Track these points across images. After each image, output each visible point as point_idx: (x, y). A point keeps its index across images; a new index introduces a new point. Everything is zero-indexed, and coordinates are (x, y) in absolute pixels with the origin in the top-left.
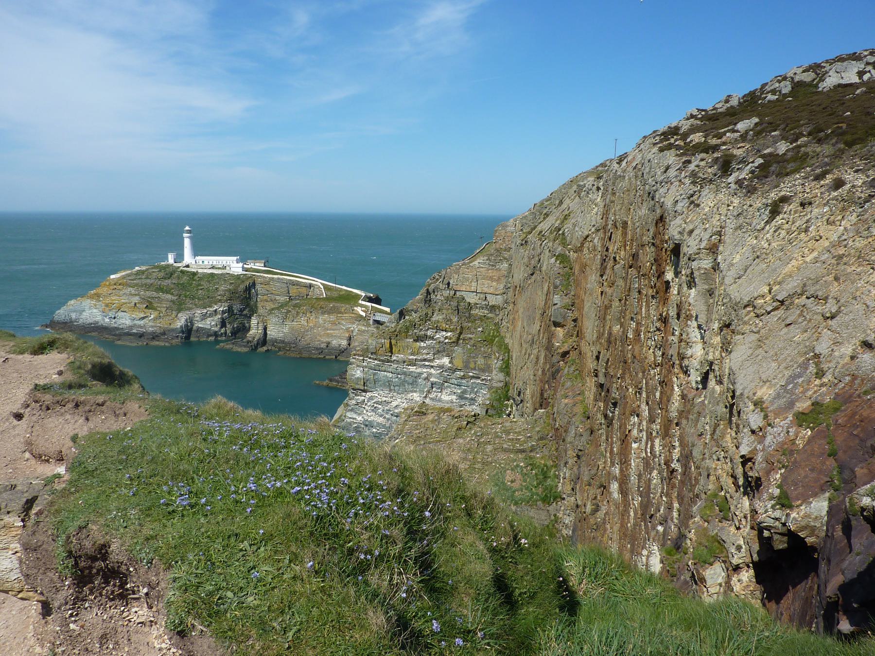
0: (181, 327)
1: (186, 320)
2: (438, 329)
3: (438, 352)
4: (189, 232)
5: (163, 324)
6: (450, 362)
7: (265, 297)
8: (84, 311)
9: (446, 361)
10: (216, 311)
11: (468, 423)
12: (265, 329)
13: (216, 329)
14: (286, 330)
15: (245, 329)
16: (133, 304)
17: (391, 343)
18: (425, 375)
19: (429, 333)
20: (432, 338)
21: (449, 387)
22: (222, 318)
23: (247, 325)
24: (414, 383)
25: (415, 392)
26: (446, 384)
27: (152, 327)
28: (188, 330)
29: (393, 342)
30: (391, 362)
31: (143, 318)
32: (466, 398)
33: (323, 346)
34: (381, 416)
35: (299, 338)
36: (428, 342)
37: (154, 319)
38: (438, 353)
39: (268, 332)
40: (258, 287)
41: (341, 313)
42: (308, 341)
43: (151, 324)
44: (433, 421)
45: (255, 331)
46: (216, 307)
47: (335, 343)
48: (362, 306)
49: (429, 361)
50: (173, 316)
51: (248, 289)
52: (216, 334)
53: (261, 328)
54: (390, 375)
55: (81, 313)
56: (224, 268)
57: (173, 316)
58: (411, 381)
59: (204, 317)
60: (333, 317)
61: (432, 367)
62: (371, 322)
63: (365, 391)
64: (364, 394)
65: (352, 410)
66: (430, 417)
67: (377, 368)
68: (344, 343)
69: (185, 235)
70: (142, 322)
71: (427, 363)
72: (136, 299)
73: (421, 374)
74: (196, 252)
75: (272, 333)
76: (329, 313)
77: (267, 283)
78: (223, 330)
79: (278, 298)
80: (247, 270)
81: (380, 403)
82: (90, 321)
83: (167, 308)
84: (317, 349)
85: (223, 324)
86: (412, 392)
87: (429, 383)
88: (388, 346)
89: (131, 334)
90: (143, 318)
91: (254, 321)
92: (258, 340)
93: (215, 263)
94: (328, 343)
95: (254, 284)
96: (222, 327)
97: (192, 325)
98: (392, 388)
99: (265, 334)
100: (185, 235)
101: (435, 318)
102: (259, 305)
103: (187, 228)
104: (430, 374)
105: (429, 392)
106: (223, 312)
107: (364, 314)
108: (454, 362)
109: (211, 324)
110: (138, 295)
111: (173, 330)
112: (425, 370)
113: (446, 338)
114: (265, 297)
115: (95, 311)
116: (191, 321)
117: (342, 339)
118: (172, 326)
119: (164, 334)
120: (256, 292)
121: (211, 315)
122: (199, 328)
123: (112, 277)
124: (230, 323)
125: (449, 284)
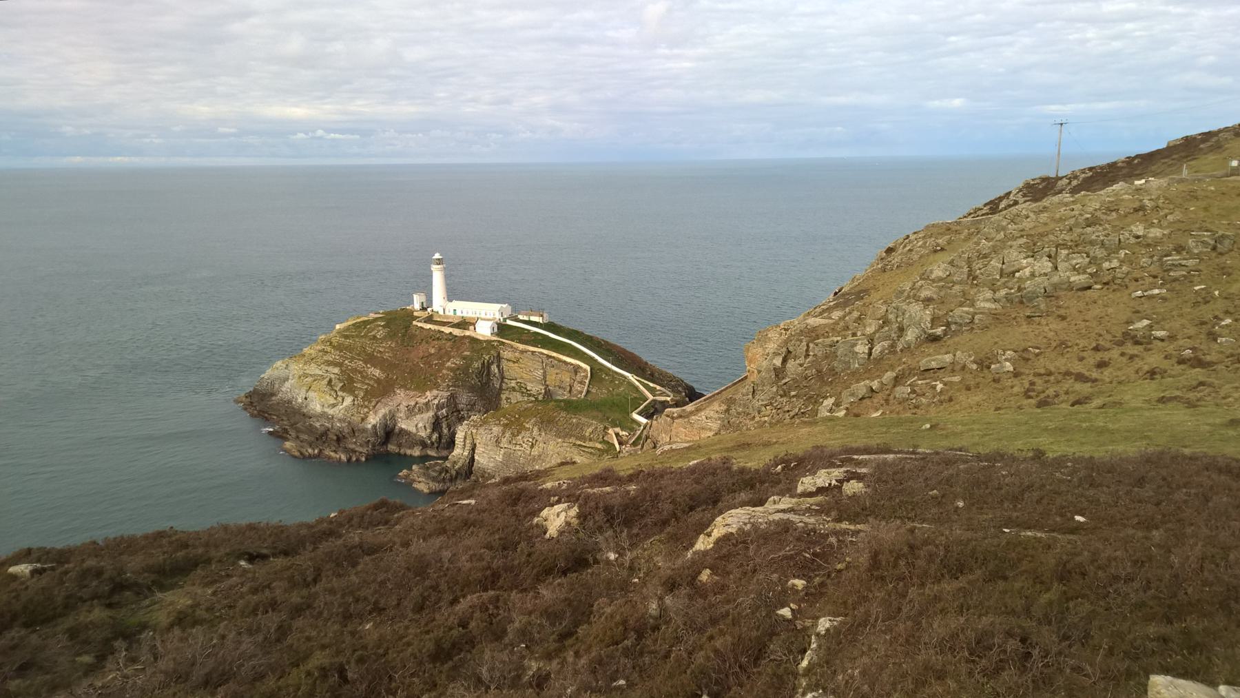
0: (374, 426)
1: (384, 416)
4: (439, 262)
8: (287, 379)
10: (427, 404)
12: (473, 449)
13: (423, 434)
16: (325, 382)
27: (340, 420)
28: (389, 432)
31: (334, 406)
39: (476, 457)
40: (504, 364)
41: (583, 438)
52: (423, 444)
53: (468, 446)
69: (435, 268)
70: (331, 412)
74: (452, 295)
75: (482, 459)
78: (435, 436)
83: (366, 391)
90: (334, 406)
95: (499, 358)
96: (433, 431)
99: (472, 459)
100: (435, 268)
103: (437, 256)
110: (340, 365)
114: (513, 384)
120: (501, 371)
121: (421, 411)
122: (402, 430)
123: (338, 327)
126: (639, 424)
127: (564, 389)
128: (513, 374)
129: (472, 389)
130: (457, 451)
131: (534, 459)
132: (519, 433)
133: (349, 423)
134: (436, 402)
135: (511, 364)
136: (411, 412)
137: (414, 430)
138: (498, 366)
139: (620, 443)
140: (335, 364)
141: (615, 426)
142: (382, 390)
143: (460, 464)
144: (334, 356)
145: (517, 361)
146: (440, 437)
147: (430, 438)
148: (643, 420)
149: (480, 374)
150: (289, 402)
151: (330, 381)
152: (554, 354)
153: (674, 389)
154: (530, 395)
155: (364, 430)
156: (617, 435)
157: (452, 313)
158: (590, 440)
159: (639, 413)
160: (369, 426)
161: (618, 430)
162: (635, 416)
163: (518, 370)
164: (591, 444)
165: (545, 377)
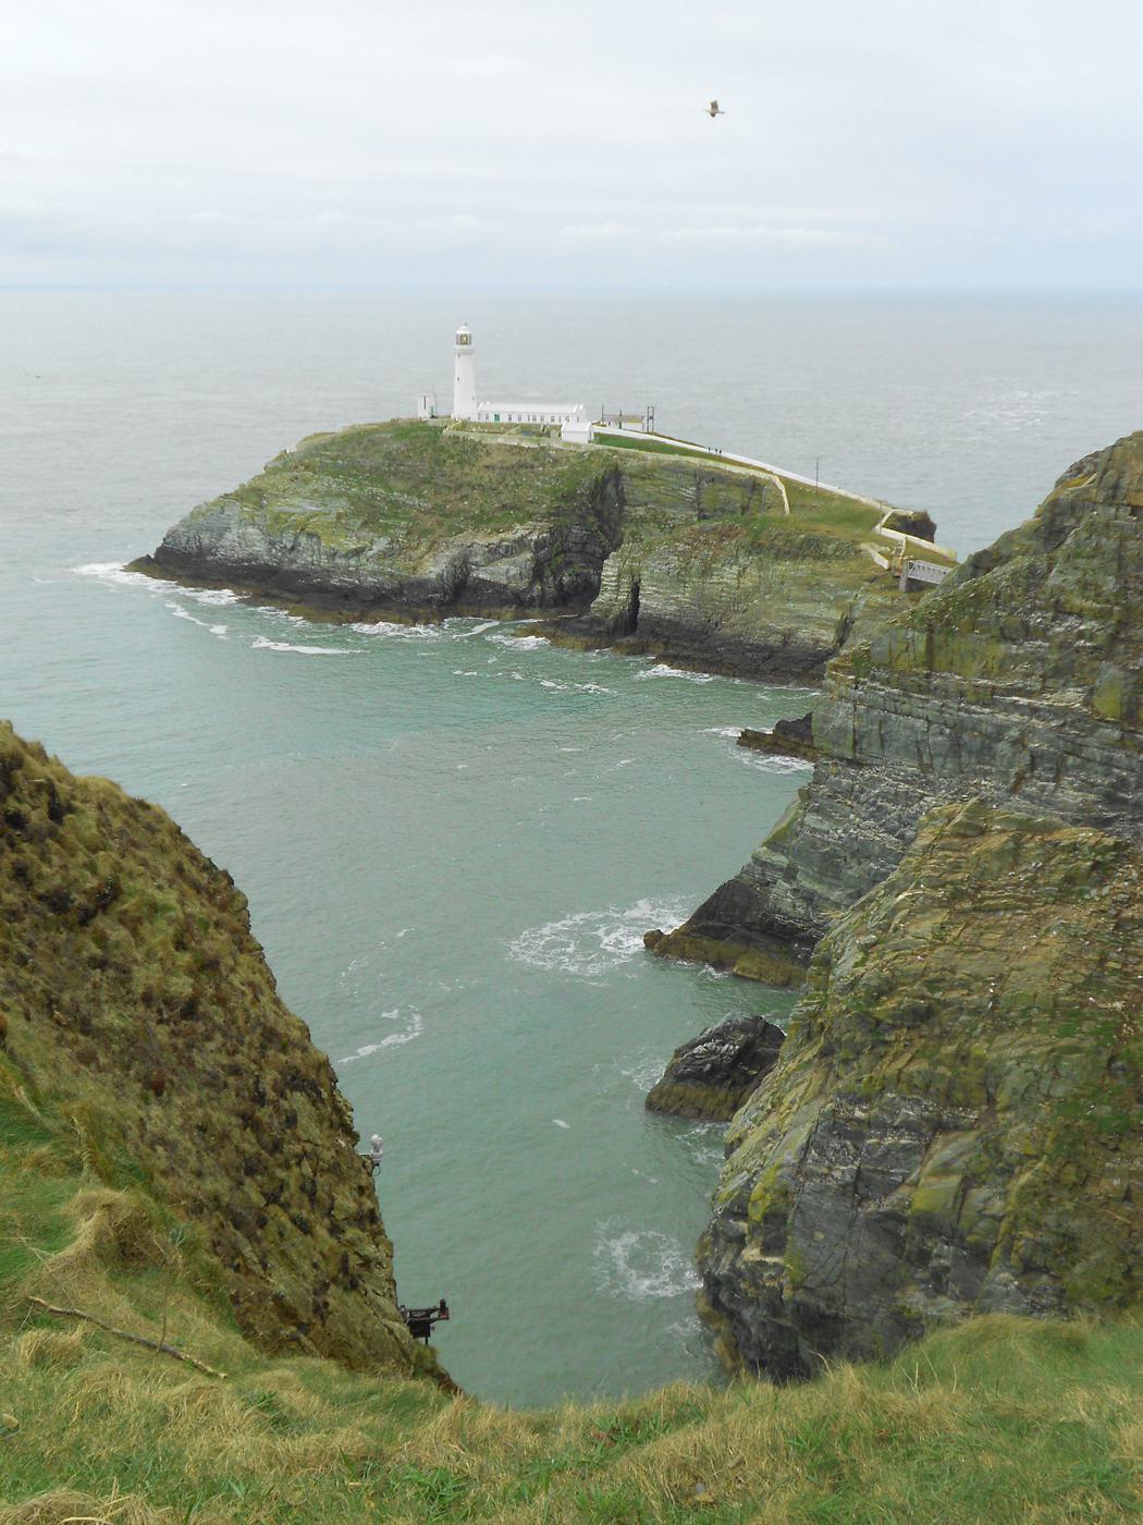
0: (440, 576)
2: (1060, 611)
3: (1057, 672)
5: (399, 568)
6: (1086, 703)
7: (641, 511)
8: (228, 529)
9: (1072, 696)
11: (1096, 866)
13: (523, 585)
14: (685, 596)
15: (591, 589)
16: (332, 518)
17: (930, 641)
18: (1014, 733)
19: (1036, 619)
20: (1043, 633)
21: (1080, 767)
23: (594, 579)
24: (985, 752)
25: (986, 774)
26: (1071, 760)
27: (374, 573)
29: (939, 639)
30: (928, 691)
31: (358, 552)
32: (1125, 801)
33: (775, 640)
34: (891, 831)
35: (715, 618)
36: (1029, 645)
37: (384, 555)
38: (1060, 674)
39: (643, 601)
41: (825, 556)
42: (738, 629)
43: (371, 566)
44: (999, 854)
45: (610, 596)
46: (520, 531)
47: (804, 634)
48: (882, 541)
49: (1029, 694)
50: (423, 549)
51: (600, 485)
53: (625, 588)
54: (920, 724)
55: (221, 535)
56: (545, 432)
57: (423, 549)
58: (977, 744)
59: (495, 553)
60: (804, 568)
61: (1034, 711)
62: (902, 584)
63: (856, 764)
64: (852, 772)
65: (817, 811)
66: (995, 842)
67: (890, 705)
68: (828, 636)
71: (1023, 701)
72: (341, 505)
73: (1001, 729)
75: (654, 601)
76: (794, 557)
77: (646, 474)
79: (670, 512)
80: (602, 438)
81: (895, 798)
82: (240, 553)
84: (757, 648)
85: (538, 573)
86: (976, 773)
87: (1025, 758)
88: (922, 647)
89: (322, 589)
91: (610, 570)
92: (616, 619)
93: (524, 421)
94: (787, 636)
96: (532, 583)
98: (926, 760)
99: (635, 604)
101: (1054, 580)
102: (627, 530)
104: (1033, 730)
105: (1020, 778)
106: (539, 545)
107: (885, 564)
108: (1096, 701)
109: (508, 572)
111: (422, 585)
112: (1015, 717)
113: (1081, 635)
114: (641, 511)
115: (250, 530)
116: (463, 565)
117: (822, 626)
118: (417, 575)
119: (399, 591)
121: (510, 552)
125: (1116, 487)
133: (392, 575)
137: (504, 581)
138: (616, 486)
151: (339, 516)
157: (492, 419)
158: (837, 558)
165: (698, 497)
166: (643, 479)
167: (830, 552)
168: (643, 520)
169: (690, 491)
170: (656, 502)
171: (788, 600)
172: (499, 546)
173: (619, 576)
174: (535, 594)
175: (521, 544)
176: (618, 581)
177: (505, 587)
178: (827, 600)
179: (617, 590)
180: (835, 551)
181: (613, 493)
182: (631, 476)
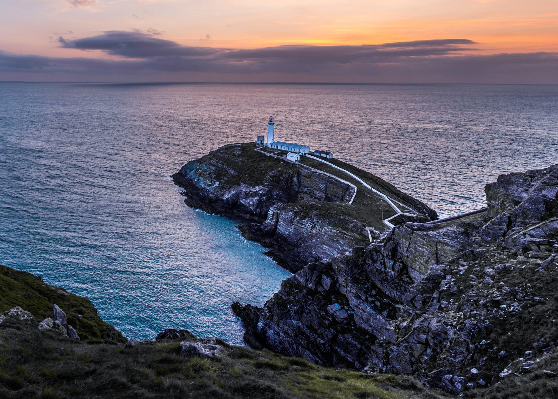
0: (227, 199)
1: (233, 195)
15: (265, 217)
22: (260, 200)
35: (300, 242)
39: (278, 227)
41: (347, 229)
52: (251, 213)
78: (258, 210)
79: (316, 192)
95: (299, 174)
96: (257, 207)
97: (239, 199)
99: (276, 227)
106: (263, 195)
114: (306, 190)
124: (266, 206)
126: (389, 228)
127: (338, 198)
128: (305, 184)
129: (281, 189)
130: (268, 221)
131: (312, 236)
132: (305, 218)
134: (261, 192)
135: (305, 179)
136: (248, 195)
137: (247, 205)
139: (373, 238)
140: (213, 165)
141: (370, 226)
142: (235, 182)
143: (269, 228)
144: (214, 161)
145: (309, 178)
146: (261, 211)
147: (255, 210)
148: (392, 226)
149: (287, 181)
150: (192, 180)
152: (333, 176)
153: (419, 210)
154: (315, 198)
155: (222, 200)
156: (372, 232)
158: (352, 231)
159: (390, 221)
160: (225, 198)
161: (371, 228)
162: (386, 222)
163: (309, 182)
164: (353, 234)
166: (307, 178)
167: (350, 227)
168: (306, 193)
169: (323, 186)
170: (311, 187)
171: (324, 244)
172: (249, 192)
173: (273, 215)
174: (257, 212)
175: (256, 194)
176: (273, 216)
177: (248, 207)
178: (339, 249)
179: (272, 220)
180: (352, 227)
181: (296, 181)
182: (304, 176)
